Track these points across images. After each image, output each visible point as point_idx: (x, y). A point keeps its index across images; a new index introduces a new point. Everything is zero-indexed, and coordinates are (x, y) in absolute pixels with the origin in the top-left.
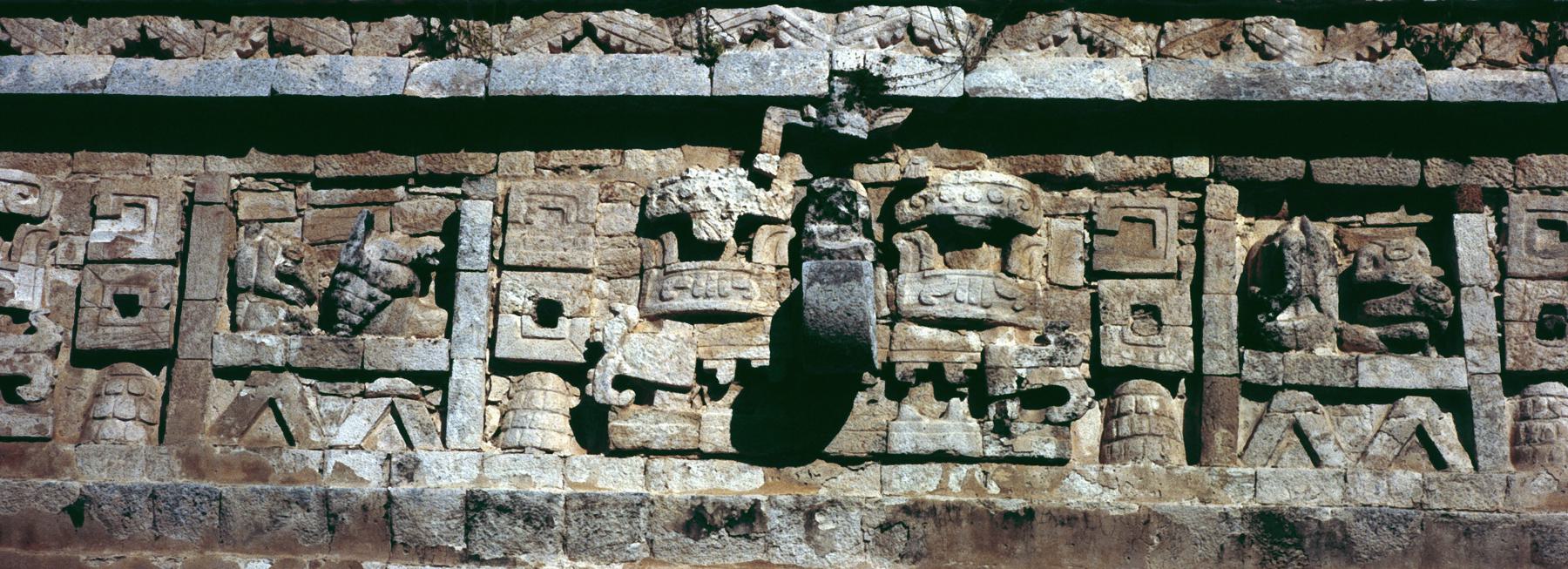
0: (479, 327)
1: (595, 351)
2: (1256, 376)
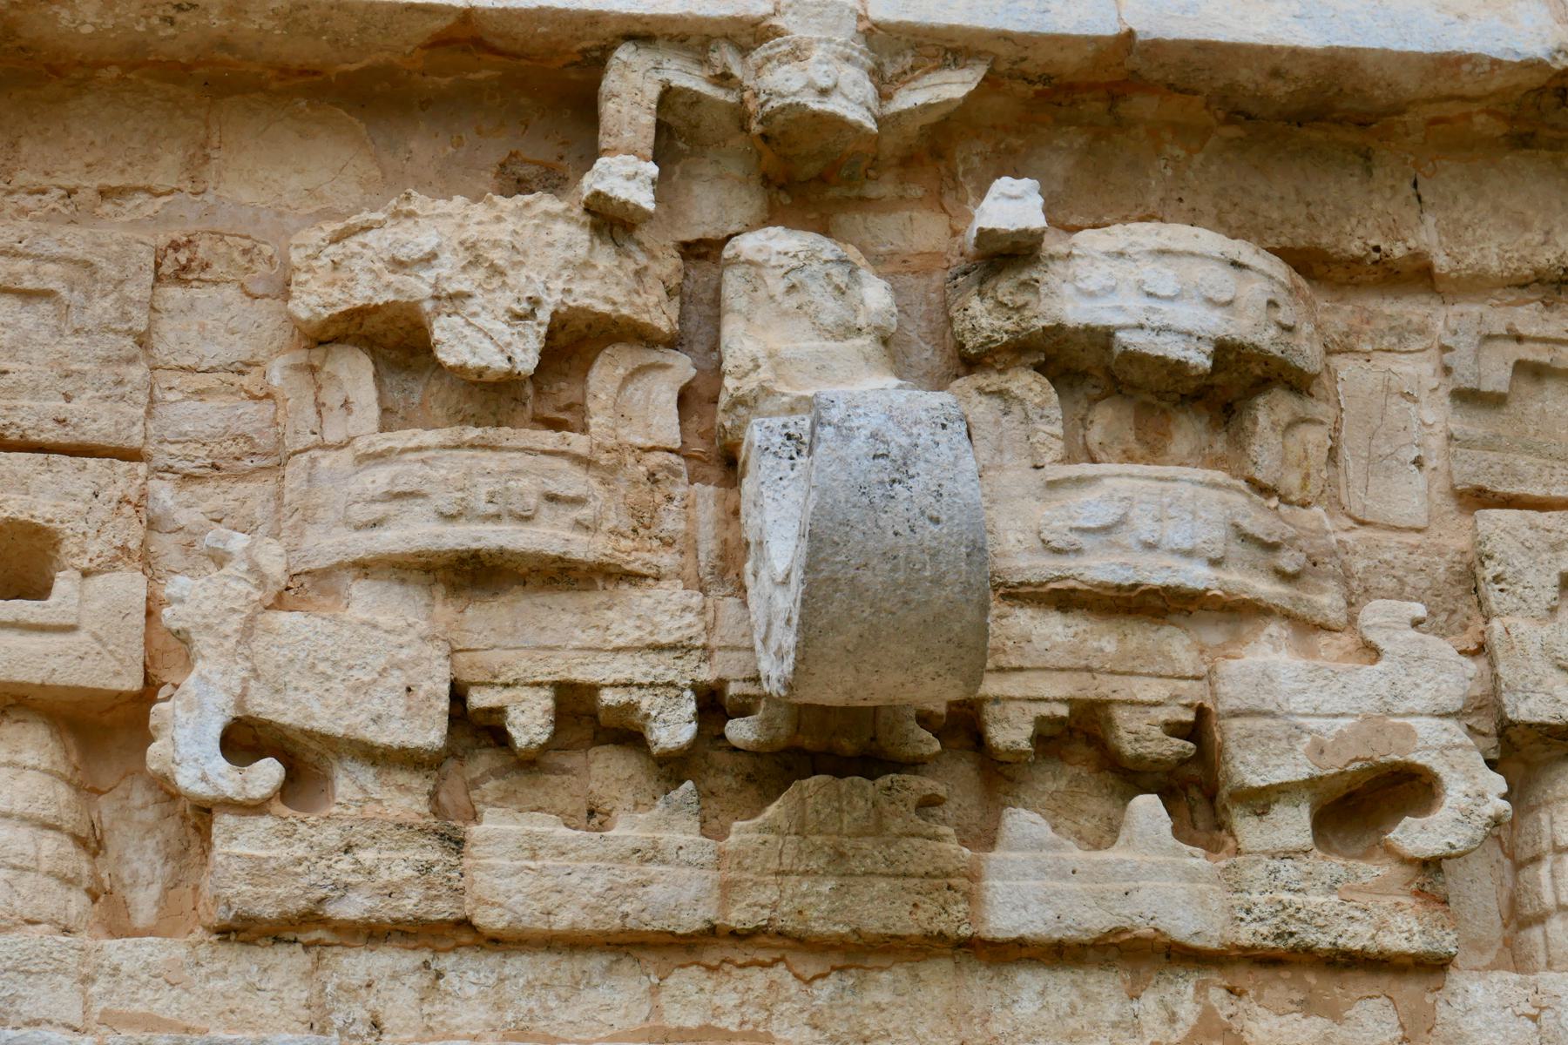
1: (165, 652)
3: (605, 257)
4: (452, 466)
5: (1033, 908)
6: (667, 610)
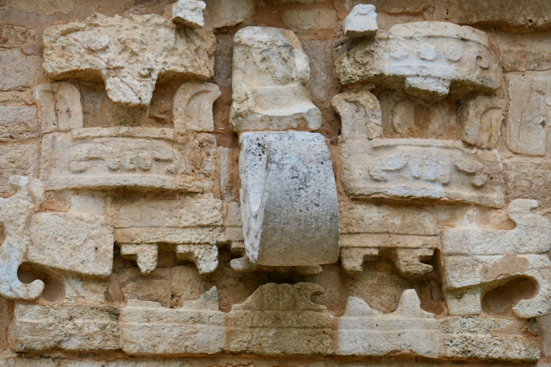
3: (182, 46)
4: (113, 147)
5: (359, 342)
6: (206, 208)
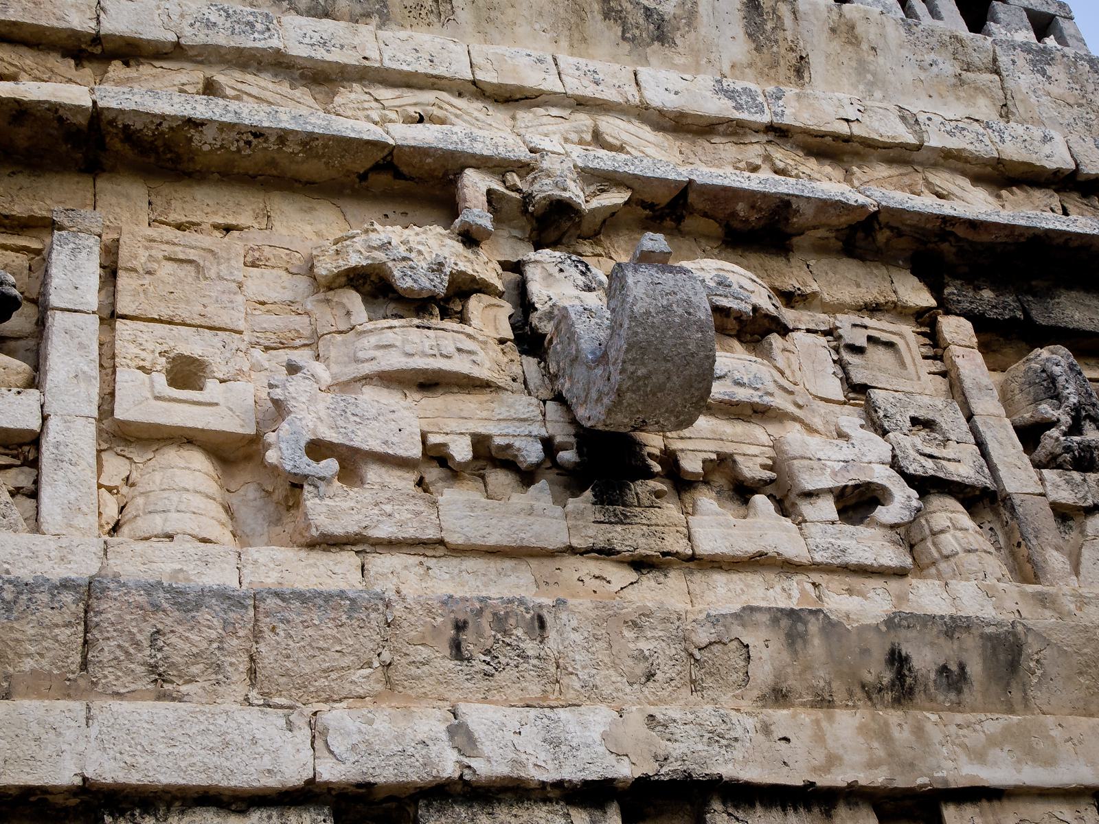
0: (88, 378)
2: (1065, 496)
